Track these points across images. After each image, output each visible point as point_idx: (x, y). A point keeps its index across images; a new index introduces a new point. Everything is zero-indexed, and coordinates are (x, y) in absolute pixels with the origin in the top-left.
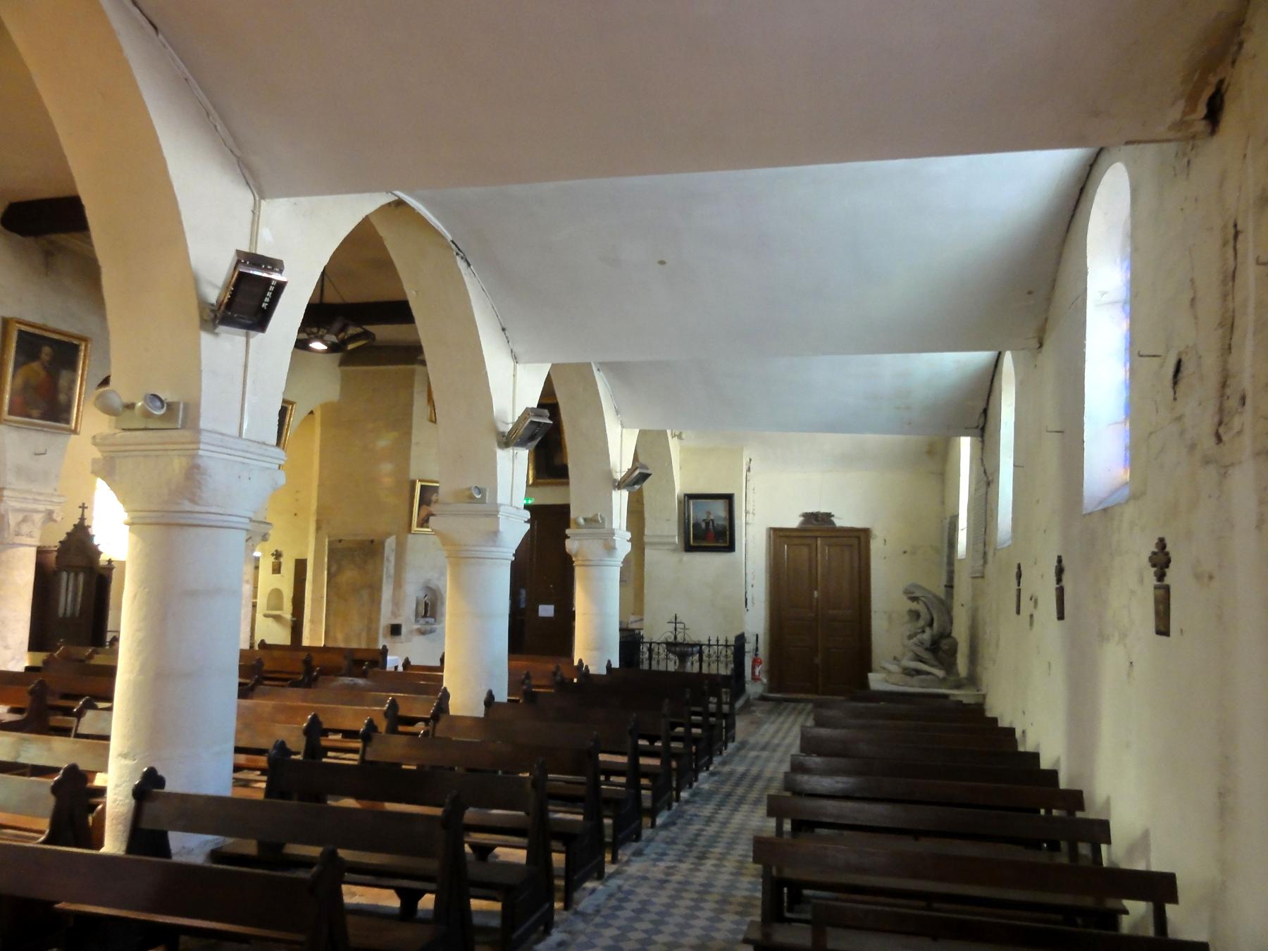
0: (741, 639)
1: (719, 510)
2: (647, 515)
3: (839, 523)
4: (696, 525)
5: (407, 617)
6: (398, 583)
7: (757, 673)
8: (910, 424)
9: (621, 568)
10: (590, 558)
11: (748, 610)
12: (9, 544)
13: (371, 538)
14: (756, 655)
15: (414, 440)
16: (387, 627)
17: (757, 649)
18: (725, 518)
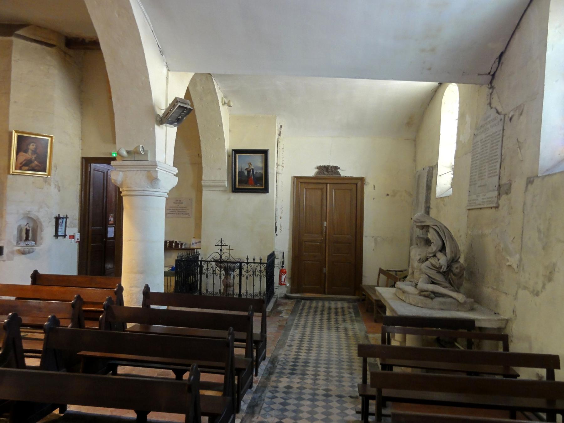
0: (272, 256)
1: (257, 162)
2: (204, 165)
3: (343, 174)
4: (240, 173)
7: (283, 280)
8: (430, 69)
9: (167, 199)
11: (277, 235)
14: (282, 267)
15: (12, 100)
17: (283, 263)
18: (262, 168)
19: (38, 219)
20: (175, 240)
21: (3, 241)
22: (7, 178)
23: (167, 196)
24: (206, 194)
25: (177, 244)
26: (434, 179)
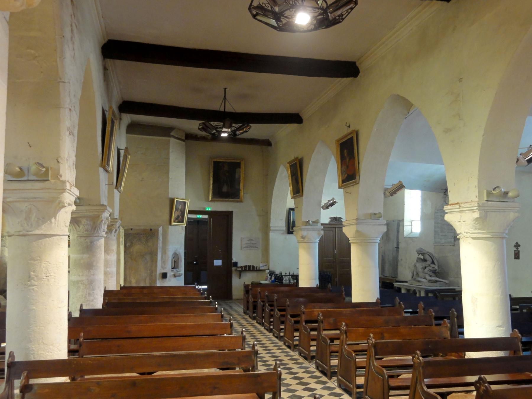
5: (168, 269)
6: (164, 252)
10: (312, 239)
12: (101, 236)
13: (150, 228)
15: (170, 176)
16: (160, 274)
19: (180, 254)
20: (252, 265)
21: (166, 269)
22: (168, 228)
23: (319, 242)
24: (272, 235)
25: (253, 267)
26: (401, 228)
